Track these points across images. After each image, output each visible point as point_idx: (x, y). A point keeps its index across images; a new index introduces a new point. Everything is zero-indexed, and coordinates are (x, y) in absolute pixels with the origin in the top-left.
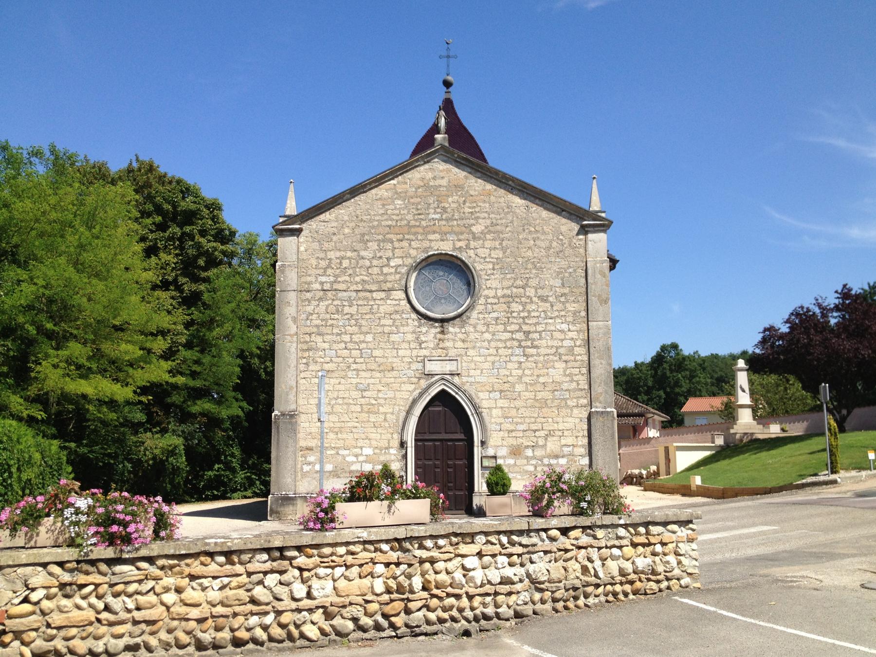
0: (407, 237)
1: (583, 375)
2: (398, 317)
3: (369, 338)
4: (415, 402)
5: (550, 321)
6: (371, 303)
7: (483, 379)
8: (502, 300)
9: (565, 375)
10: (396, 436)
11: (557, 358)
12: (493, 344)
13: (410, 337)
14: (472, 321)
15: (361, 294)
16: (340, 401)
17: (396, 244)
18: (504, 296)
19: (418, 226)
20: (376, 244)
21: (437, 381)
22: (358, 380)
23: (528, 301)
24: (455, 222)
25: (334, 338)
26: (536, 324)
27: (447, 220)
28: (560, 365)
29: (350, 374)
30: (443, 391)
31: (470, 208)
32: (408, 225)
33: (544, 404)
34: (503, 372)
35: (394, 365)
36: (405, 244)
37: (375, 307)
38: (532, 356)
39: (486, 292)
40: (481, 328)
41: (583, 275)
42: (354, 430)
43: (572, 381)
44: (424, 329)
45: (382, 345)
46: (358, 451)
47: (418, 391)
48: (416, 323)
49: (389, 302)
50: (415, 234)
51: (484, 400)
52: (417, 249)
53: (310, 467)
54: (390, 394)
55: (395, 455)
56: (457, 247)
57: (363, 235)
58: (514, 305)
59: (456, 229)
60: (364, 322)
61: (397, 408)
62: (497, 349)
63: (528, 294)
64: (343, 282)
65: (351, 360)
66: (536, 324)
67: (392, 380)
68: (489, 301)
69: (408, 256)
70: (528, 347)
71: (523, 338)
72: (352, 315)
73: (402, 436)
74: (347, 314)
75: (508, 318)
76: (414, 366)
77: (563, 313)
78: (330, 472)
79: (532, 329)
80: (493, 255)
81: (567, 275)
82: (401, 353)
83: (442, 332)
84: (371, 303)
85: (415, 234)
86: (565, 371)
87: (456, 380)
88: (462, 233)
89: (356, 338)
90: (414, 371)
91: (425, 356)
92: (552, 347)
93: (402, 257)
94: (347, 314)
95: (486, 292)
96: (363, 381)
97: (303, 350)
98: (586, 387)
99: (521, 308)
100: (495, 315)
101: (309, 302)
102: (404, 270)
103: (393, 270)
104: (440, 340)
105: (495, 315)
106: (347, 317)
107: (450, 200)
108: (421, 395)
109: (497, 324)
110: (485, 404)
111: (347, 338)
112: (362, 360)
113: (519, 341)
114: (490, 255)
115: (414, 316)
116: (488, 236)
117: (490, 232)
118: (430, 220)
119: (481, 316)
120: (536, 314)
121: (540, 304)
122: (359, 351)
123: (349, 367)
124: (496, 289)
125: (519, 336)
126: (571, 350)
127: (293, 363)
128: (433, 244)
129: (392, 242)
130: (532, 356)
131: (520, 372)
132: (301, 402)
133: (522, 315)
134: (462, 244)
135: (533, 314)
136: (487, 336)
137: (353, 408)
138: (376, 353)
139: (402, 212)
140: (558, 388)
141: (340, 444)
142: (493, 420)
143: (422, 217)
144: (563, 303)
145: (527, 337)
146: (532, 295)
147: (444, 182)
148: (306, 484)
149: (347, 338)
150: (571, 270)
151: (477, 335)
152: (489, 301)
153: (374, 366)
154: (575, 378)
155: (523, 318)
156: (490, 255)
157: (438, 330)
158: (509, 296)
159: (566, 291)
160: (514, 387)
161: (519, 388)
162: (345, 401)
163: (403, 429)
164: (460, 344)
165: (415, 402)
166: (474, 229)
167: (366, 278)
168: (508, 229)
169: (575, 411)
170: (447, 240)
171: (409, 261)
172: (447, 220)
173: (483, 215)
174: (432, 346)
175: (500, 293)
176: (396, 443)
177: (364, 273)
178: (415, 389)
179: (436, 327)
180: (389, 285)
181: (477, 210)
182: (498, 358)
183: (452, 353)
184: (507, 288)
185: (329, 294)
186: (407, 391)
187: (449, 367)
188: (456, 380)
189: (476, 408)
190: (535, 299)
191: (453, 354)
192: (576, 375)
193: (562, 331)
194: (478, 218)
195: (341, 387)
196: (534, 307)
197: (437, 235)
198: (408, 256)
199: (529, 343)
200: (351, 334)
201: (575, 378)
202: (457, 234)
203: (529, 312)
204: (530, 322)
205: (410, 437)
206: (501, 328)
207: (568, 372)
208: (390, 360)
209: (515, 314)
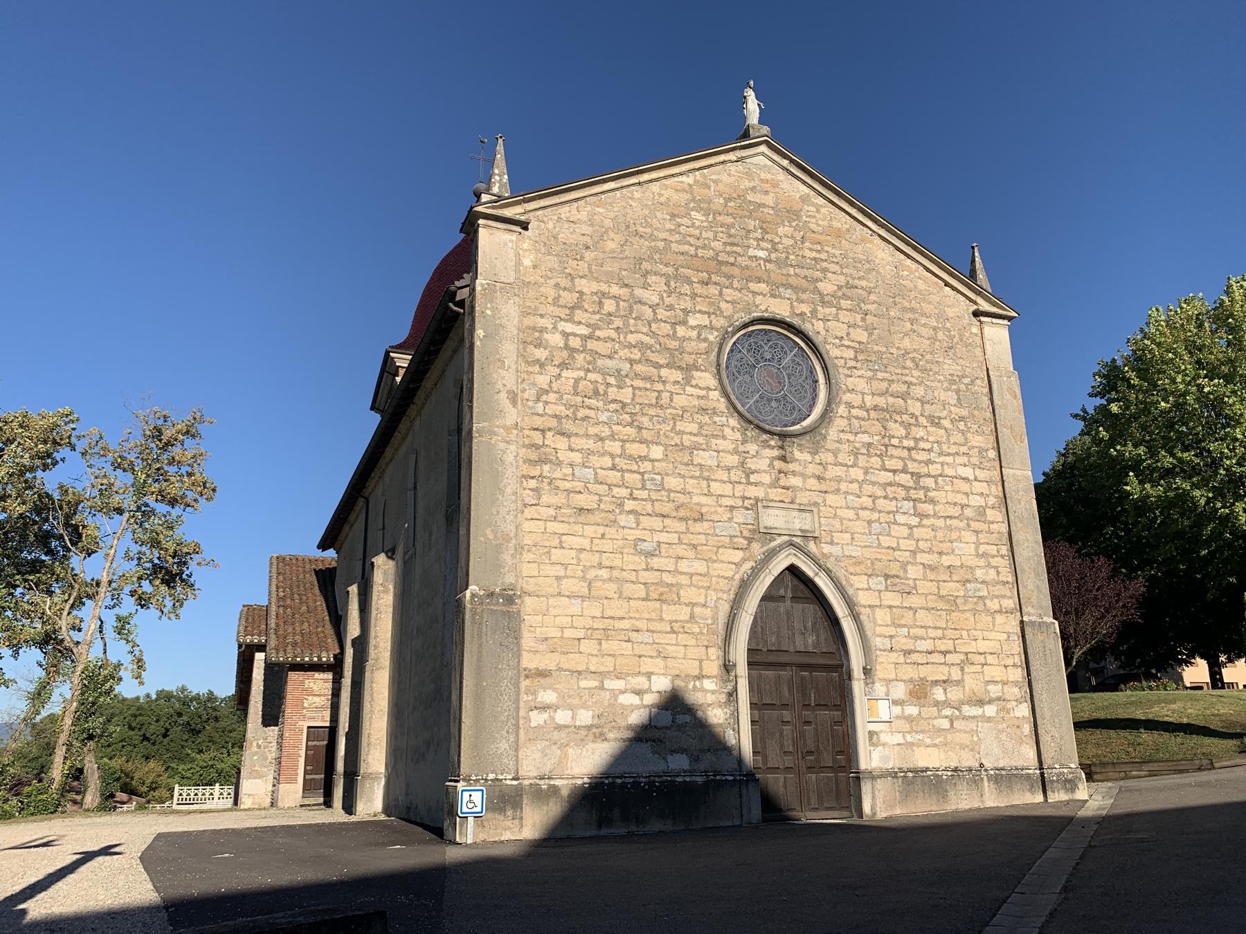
0: (715, 278)
1: (1002, 557)
2: (706, 419)
3: (657, 452)
4: (745, 586)
5: (949, 459)
6: (660, 387)
7: (857, 552)
8: (873, 414)
9: (977, 555)
10: (714, 653)
11: (962, 524)
12: (868, 489)
13: (733, 460)
14: (830, 444)
15: (639, 368)
16: (604, 573)
17: (699, 289)
18: (876, 408)
19: (732, 264)
20: (663, 280)
21: (781, 547)
22: (638, 534)
23: (912, 421)
24: (791, 271)
25: (590, 444)
26: (928, 462)
27: (777, 262)
28: (969, 537)
29: (623, 520)
30: (792, 570)
31: (811, 250)
32: (715, 258)
33: (952, 603)
34: (886, 541)
35: (704, 510)
36: (714, 290)
37: (665, 395)
38: (927, 516)
39: (847, 397)
40: (842, 458)
41: (987, 390)
42: (634, 635)
43: (989, 565)
44: (752, 448)
45: (682, 470)
46: (641, 682)
47: (748, 565)
48: (738, 436)
49: (689, 390)
50: (729, 277)
51: (865, 590)
52: (733, 302)
53: (546, 716)
54: (700, 567)
56: (798, 312)
57: (640, 260)
58: (891, 425)
59: (792, 280)
60: (645, 421)
61: (713, 595)
62: (874, 497)
63: (911, 410)
64: (606, 340)
65: (624, 492)
66: (928, 462)
67: (702, 539)
68: (855, 412)
69: (718, 312)
70: (920, 500)
71: (911, 484)
72: (624, 405)
73: (726, 652)
74: (614, 401)
75: (886, 446)
76: (739, 517)
77: (964, 449)
78: (589, 728)
79: (924, 470)
80: (853, 336)
81: (963, 387)
82: (716, 487)
83: (783, 459)
84: (660, 387)
85: (729, 277)
86: (977, 549)
88: (804, 291)
89: (635, 449)
90: (739, 524)
91: (757, 500)
92: (955, 504)
93: (709, 313)
94: (614, 401)
95: (847, 397)
96: (646, 535)
97: (529, 461)
98: (1010, 579)
99: (903, 432)
100: (865, 438)
101: (542, 366)
102: (713, 337)
103: (694, 334)
104: (780, 472)
105: (865, 438)
106: (613, 406)
107: (781, 230)
108: (756, 572)
109: (869, 455)
111: (615, 447)
112: (644, 494)
113: (907, 489)
114: (848, 334)
115: (733, 422)
116: (845, 303)
117: (845, 297)
118: (750, 258)
119: (844, 436)
120: (927, 446)
121: (930, 429)
122: (639, 476)
123: (621, 505)
124: (863, 394)
125: (904, 479)
126: (981, 511)
127: (510, 484)
128: (759, 299)
129: (690, 283)
130: (927, 516)
131: (911, 544)
132: (528, 569)
133: (906, 443)
134: (805, 308)
135: (922, 445)
136: (856, 473)
137: (629, 589)
138: (673, 482)
139: (704, 235)
140: (970, 577)
141: (609, 664)
143: (738, 249)
144: (963, 432)
145: (917, 482)
146: (918, 413)
147: (769, 200)
148: (537, 755)
149: (615, 447)
150: (967, 381)
151: (839, 471)
152: (855, 412)
153: (667, 508)
154: (994, 562)
155: (909, 449)
156: (848, 334)
157: (776, 453)
158: (883, 410)
159: (964, 413)
160: (906, 571)
161: (913, 572)
162: (616, 573)
164: (812, 482)
166: (820, 285)
167: (646, 339)
168: (873, 297)
169: (1000, 619)
170: (780, 296)
171: (720, 322)
172: (777, 262)
173: (833, 267)
174: (766, 479)
175: (869, 402)
176: (713, 667)
177: (645, 330)
178: (744, 560)
179: (773, 448)
180: (689, 359)
181: (824, 256)
182: (876, 516)
183: (803, 498)
184: (880, 395)
185: (580, 358)
186: (730, 564)
187: (799, 522)
188: (812, 546)
189: (850, 604)
190: (922, 420)
191: (805, 501)
192: (993, 556)
193: (965, 479)
194: (825, 270)
195: (607, 545)
196: (921, 433)
197: (763, 286)
198: (718, 312)
199: (921, 494)
200: (623, 441)
201: (994, 562)
202: (795, 289)
203: (916, 440)
204: (919, 458)
205: (740, 656)
206: (876, 461)
207: (982, 549)
208: (696, 499)
209: (895, 441)
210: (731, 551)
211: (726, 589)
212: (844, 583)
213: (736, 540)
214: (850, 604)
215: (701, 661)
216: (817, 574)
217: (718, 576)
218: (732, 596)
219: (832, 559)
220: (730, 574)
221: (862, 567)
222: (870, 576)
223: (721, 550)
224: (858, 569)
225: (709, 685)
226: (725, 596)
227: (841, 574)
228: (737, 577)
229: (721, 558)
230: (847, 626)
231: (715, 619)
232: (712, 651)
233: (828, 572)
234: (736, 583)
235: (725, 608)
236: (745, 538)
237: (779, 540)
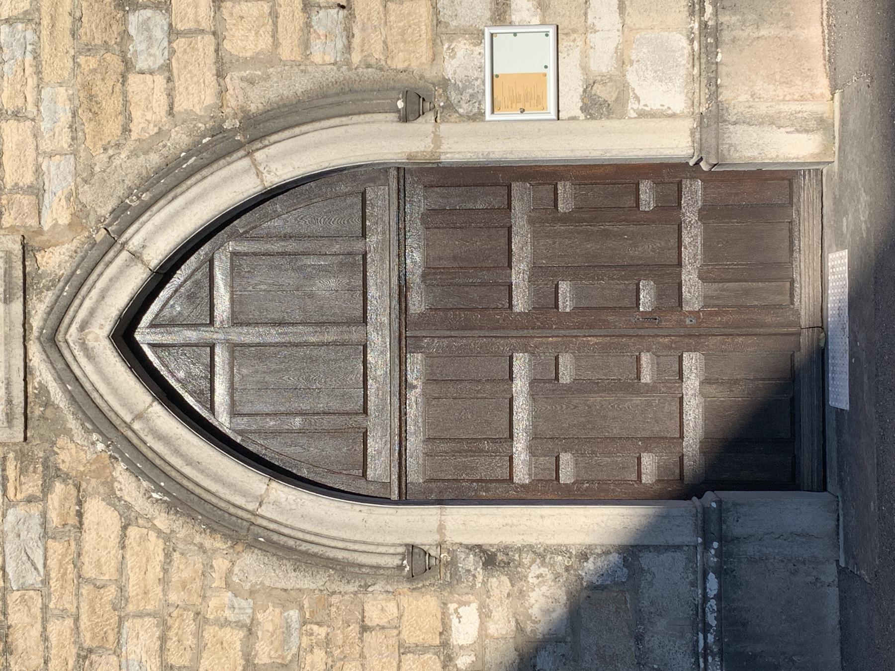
4: (186, 500)
7: (58, 104)
10: (379, 607)
21: (68, 376)
47: (128, 487)
55: (485, 614)
61: (219, 603)
67: (59, 629)
87: (55, 261)
110: (197, 96)
142: (288, 50)
163: (343, 569)
165: (186, 500)
176: (418, 610)
178: (112, 498)
186: (124, 541)
188: (55, 261)
189: (222, 143)
210: (89, 538)
211: (198, 560)
212: (155, 159)
213: (54, 519)
214: (222, 143)
215: (404, 649)
216: (136, 256)
217: (165, 581)
218: (217, 543)
219: (87, 195)
220: (155, 545)
221: (101, 89)
222: (128, 65)
223: (89, 571)
224: (111, 105)
225: (465, 628)
226: (221, 564)
227: (129, 167)
228: (162, 521)
229: (109, 572)
230: (287, 159)
231: (286, 598)
232: (374, 616)
233: (127, 215)
234: (182, 529)
235: (252, 566)
236: (46, 488)
237: (43, 373)
